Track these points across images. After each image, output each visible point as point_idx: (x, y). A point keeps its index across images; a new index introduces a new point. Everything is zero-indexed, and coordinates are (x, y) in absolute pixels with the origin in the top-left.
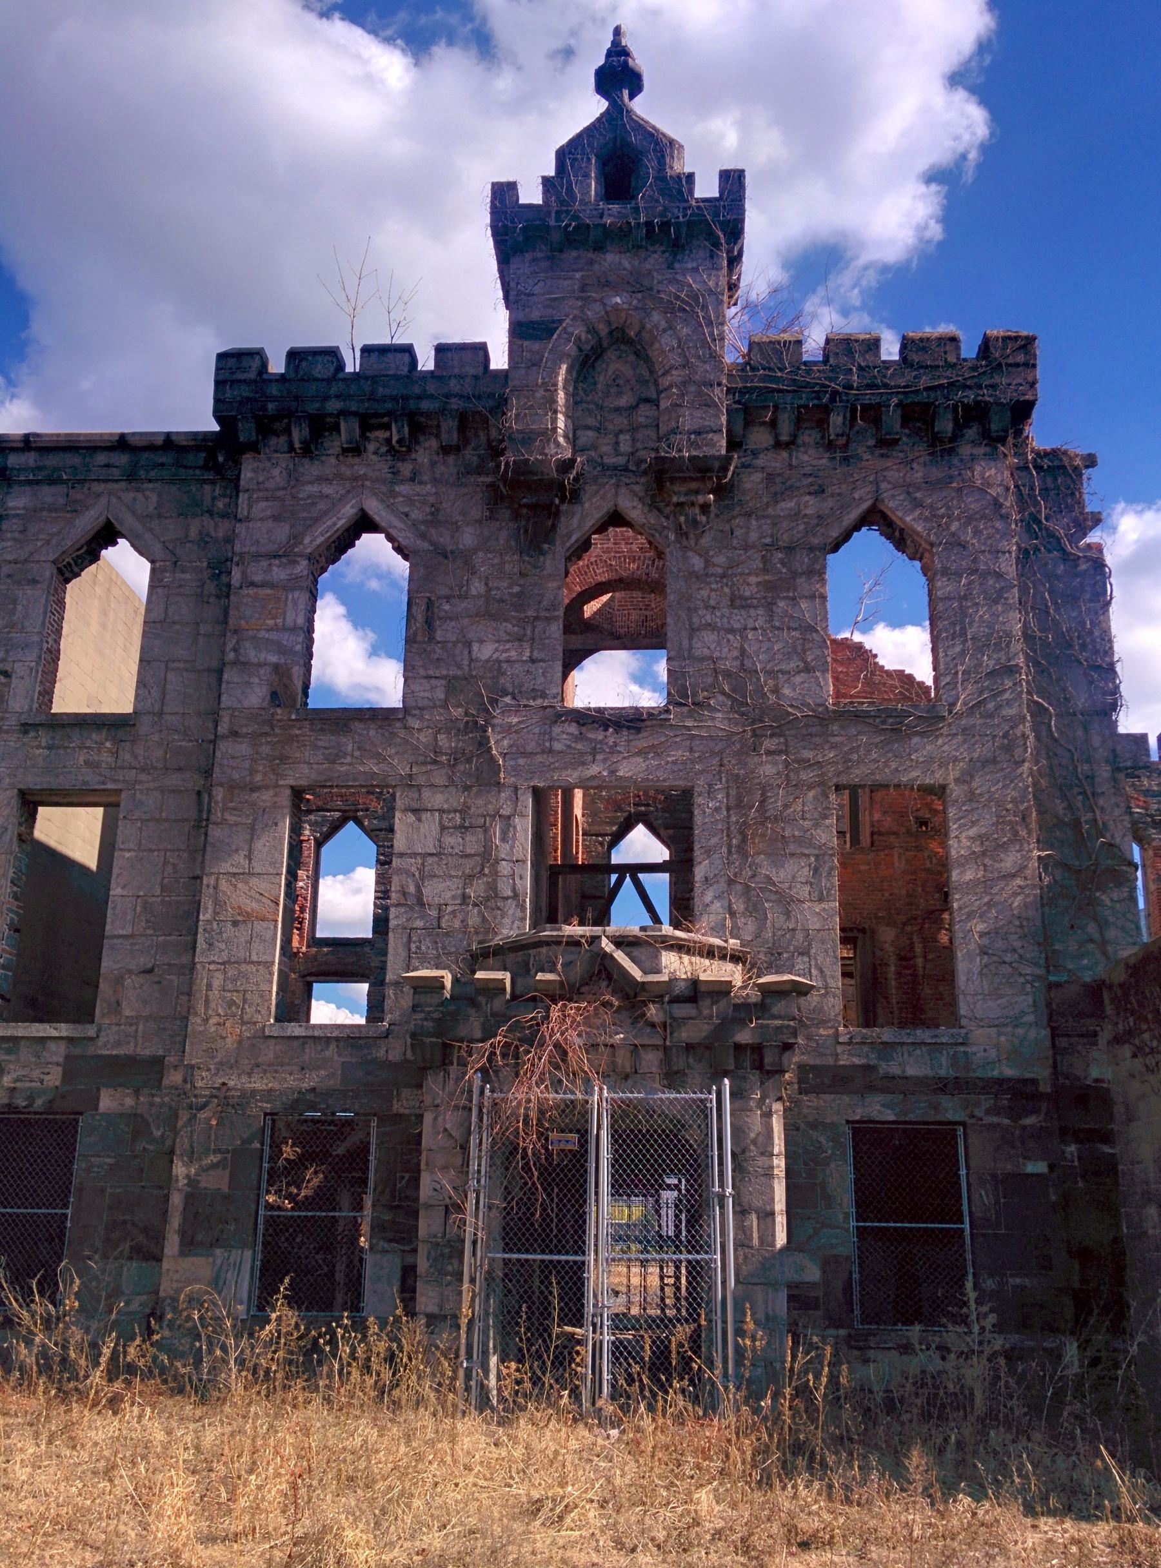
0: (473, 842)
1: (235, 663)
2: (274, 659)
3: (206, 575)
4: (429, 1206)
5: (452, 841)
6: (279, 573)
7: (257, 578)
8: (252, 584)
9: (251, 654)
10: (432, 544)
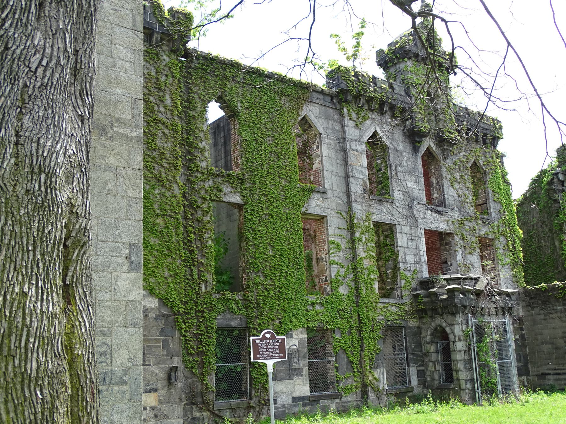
0: (414, 243)
1: (352, 177)
2: (362, 177)
3: (336, 142)
4: (460, 351)
5: (410, 243)
6: (359, 148)
7: (354, 148)
8: (352, 150)
9: (356, 174)
10: (394, 147)
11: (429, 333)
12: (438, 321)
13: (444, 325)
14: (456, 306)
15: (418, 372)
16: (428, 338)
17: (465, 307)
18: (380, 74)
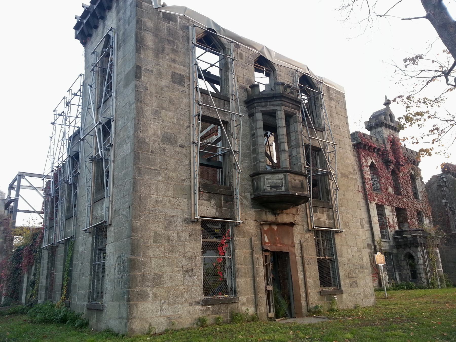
11: (403, 256)
12: (408, 250)
13: (411, 252)
14: (418, 243)
15: (399, 274)
16: (402, 258)
17: (421, 244)
18: (368, 133)
